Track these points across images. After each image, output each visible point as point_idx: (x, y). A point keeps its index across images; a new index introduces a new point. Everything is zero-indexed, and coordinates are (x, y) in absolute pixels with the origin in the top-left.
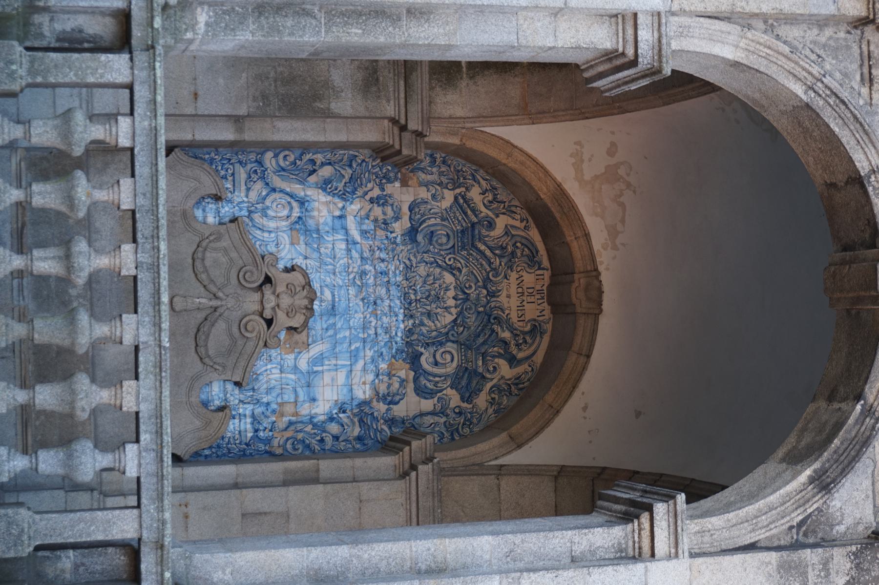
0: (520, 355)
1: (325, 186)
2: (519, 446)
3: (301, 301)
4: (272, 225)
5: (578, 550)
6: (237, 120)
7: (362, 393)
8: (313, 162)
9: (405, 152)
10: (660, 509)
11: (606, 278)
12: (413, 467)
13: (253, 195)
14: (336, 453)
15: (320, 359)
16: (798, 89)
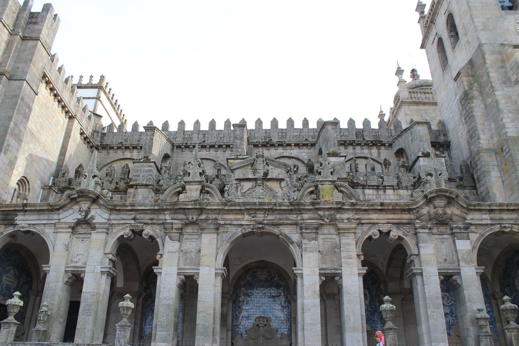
0: (274, 275)
1: (240, 313)
2: (290, 278)
3: (262, 319)
4: (247, 324)
5: (301, 286)
6: (228, 330)
7: (280, 307)
8: (235, 315)
9: (234, 298)
10: (295, 272)
11: (259, 260)
12: (293, 299)
13: (241, 327)
14: (291, 313)
15: (273, 315)
16: (228, 244)
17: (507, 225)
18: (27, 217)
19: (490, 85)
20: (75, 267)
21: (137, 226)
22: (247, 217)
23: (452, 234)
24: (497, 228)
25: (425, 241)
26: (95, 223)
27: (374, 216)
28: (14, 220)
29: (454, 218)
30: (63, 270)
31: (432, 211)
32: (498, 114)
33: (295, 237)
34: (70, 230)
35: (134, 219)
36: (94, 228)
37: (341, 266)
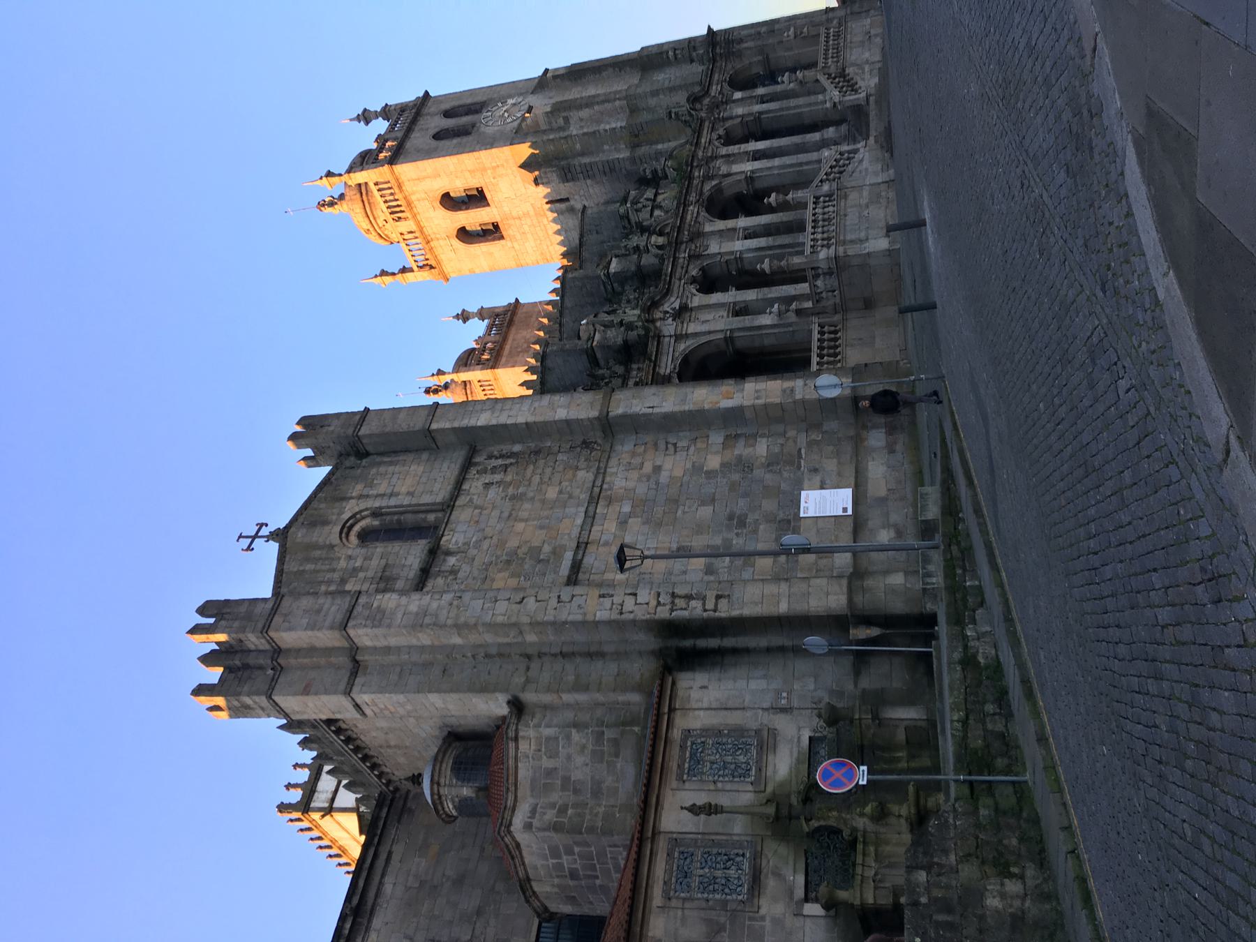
18: (663, 365)
19: (562, 141)
20: (728, 312)
22: (691, 208)
23: (726, 103)
24: (726, 85)
27: (703, 141)
30: (731, 319)
32: (598, 136)
33: (714, 183)
34: (685, 325)
35: (680, 279)
36: (686, 304)
37: (747, 152)
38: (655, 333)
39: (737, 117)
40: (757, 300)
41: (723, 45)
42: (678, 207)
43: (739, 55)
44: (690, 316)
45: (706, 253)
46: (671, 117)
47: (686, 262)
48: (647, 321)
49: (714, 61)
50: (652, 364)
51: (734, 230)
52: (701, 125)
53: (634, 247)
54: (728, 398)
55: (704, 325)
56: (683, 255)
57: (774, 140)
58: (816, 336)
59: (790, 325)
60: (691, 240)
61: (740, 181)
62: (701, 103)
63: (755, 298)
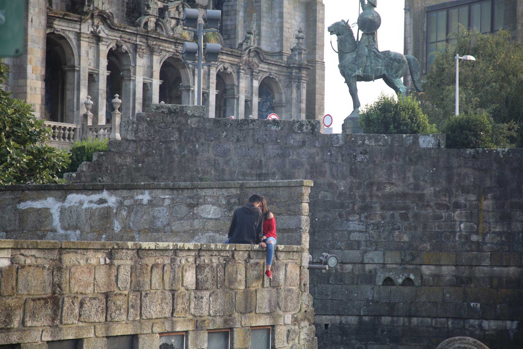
17: (273, 74)
18: (60, 23)
20: (92, 70)
21: (120, 42)
22: (173, 47)
23: (252, 75)
24: (267, 75)
25: (242, 79)
26: (103, 37)
27: (224, 57)
28: (53, 24)
29: (255, 65)
30: (87, 71)
31: (248, 58)
34: (87, 40)
35: (121, 37)
37: (209, 88)
38: (84, 19)
39: (239, 82)
40: (98, 89)
41: (298, 75)
42: (174, 38)
43: (289, 86)
44: (93, 43)
45: (137, 56)
46: (249, 33)
47: (133, 42)
48: (92, 15)
49: (288, 67)
50: (61, 16)
51: (151, 76)
52: (237, 56)
53: (149, 5)
54: (33, 70)
55: (86, 53)
56: (138, 41)
57: (214, 107)
58: (68, 126)
59: (78, 109)
60: (148, 46)
61: (189, 82)
62: (255, 56)
63: (100, 88)
